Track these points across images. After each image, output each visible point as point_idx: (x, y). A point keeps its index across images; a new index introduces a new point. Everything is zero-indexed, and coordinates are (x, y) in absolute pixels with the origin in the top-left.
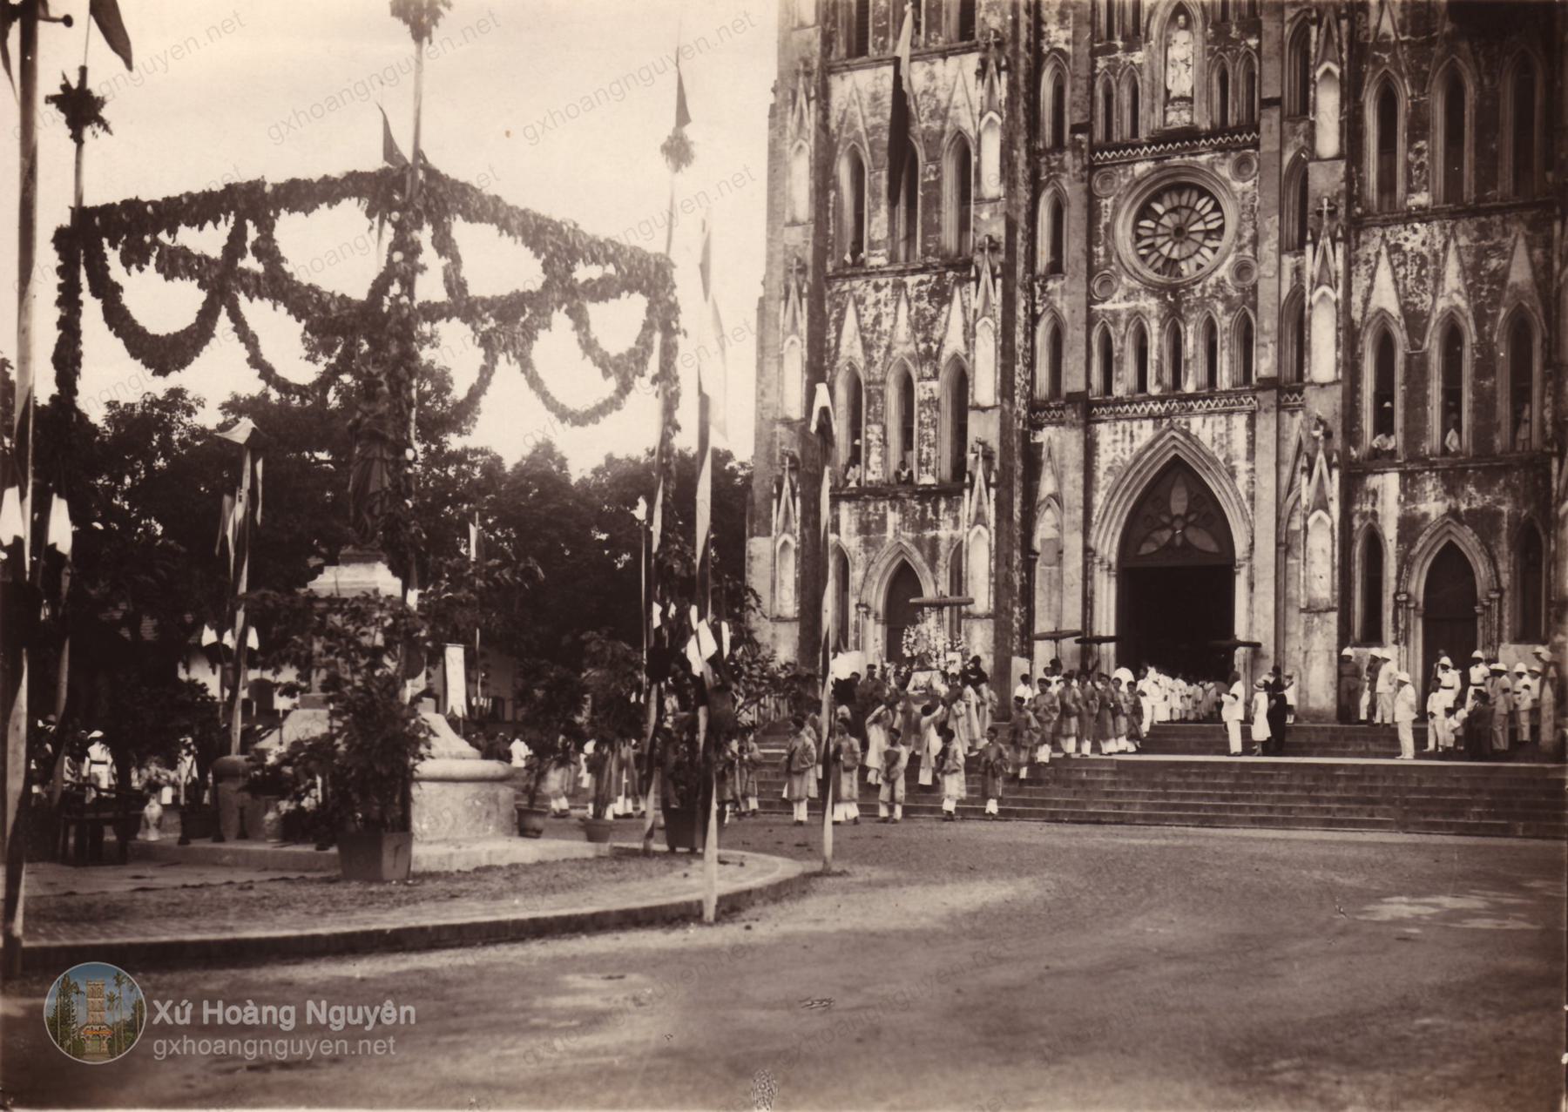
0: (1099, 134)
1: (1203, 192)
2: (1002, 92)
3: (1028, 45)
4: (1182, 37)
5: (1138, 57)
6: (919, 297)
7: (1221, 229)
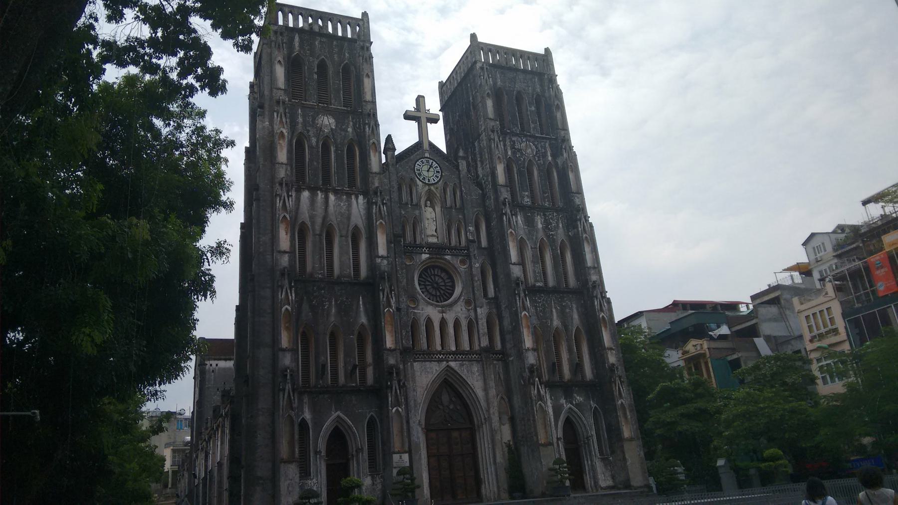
4: (430, 210)
5: (417, 212)
7: (453, 287)
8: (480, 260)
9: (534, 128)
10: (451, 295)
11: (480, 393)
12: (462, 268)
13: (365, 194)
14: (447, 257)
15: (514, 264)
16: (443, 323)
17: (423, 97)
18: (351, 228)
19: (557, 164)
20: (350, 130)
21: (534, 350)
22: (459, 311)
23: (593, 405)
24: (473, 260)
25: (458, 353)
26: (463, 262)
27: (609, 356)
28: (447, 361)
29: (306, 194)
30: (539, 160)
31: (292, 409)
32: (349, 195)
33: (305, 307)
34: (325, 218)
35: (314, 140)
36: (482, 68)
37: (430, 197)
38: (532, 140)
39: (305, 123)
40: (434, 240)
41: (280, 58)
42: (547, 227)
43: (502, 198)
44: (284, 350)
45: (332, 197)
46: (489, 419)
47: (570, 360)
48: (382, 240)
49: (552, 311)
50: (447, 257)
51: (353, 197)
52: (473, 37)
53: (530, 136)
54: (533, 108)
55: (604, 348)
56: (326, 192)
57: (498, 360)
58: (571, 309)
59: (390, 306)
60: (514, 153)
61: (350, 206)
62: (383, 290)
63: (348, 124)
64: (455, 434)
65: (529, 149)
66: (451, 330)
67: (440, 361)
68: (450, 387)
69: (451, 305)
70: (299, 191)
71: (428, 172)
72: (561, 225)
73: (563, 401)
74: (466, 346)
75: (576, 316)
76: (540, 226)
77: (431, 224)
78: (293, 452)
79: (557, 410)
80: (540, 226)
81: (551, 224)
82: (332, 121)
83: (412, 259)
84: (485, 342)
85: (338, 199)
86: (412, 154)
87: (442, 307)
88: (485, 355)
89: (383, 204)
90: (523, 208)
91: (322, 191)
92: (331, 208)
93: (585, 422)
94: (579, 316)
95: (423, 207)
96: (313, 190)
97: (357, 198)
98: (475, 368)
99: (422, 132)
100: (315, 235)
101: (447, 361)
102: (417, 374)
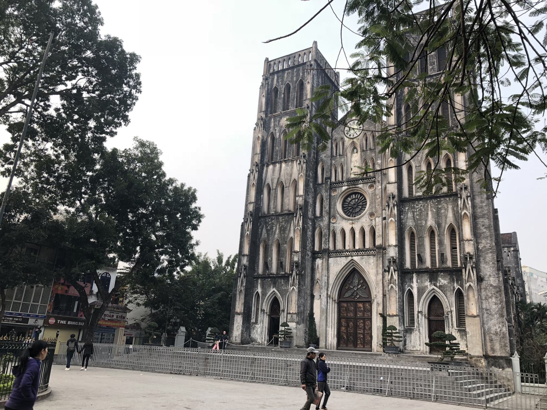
0: (333, 180)
2: (304, 166)
3: (314, 157)
5: (343, 160)
6: (282, 222)
7: (366, 204)
9: (432, 68)
12: (371, 191)
14: (360, 186)
15: (392, 183)
16: (353, 231)
21: (395, 246)
23: (457, 286)
24: (377, 184)
25: (363, 251)
26: (371, 187)
29: (271, 167)
35: (278, 134)
37: (354, 147)
39: (274, 127)
41: (264, 94)
44: (244, 256)
45: (283, 165)
49: (427, 214)
50: (360, 186)
51: (295, 162)
55: (463, 240)
58: (447, 210)
61: (292, 168)
62: (296, 216)
64: (361, 305)
67: (347, 256)
69: (358, 219)
70: (268, 166)
73: (427, 283)
75: (450, 215)
79: (421, 291)
84: (379, 242)
87: (352, 220)
89: (304, 163)
95: (349, 155)
96: (274, 164)
97: (297, 161)
101: (352, 256)
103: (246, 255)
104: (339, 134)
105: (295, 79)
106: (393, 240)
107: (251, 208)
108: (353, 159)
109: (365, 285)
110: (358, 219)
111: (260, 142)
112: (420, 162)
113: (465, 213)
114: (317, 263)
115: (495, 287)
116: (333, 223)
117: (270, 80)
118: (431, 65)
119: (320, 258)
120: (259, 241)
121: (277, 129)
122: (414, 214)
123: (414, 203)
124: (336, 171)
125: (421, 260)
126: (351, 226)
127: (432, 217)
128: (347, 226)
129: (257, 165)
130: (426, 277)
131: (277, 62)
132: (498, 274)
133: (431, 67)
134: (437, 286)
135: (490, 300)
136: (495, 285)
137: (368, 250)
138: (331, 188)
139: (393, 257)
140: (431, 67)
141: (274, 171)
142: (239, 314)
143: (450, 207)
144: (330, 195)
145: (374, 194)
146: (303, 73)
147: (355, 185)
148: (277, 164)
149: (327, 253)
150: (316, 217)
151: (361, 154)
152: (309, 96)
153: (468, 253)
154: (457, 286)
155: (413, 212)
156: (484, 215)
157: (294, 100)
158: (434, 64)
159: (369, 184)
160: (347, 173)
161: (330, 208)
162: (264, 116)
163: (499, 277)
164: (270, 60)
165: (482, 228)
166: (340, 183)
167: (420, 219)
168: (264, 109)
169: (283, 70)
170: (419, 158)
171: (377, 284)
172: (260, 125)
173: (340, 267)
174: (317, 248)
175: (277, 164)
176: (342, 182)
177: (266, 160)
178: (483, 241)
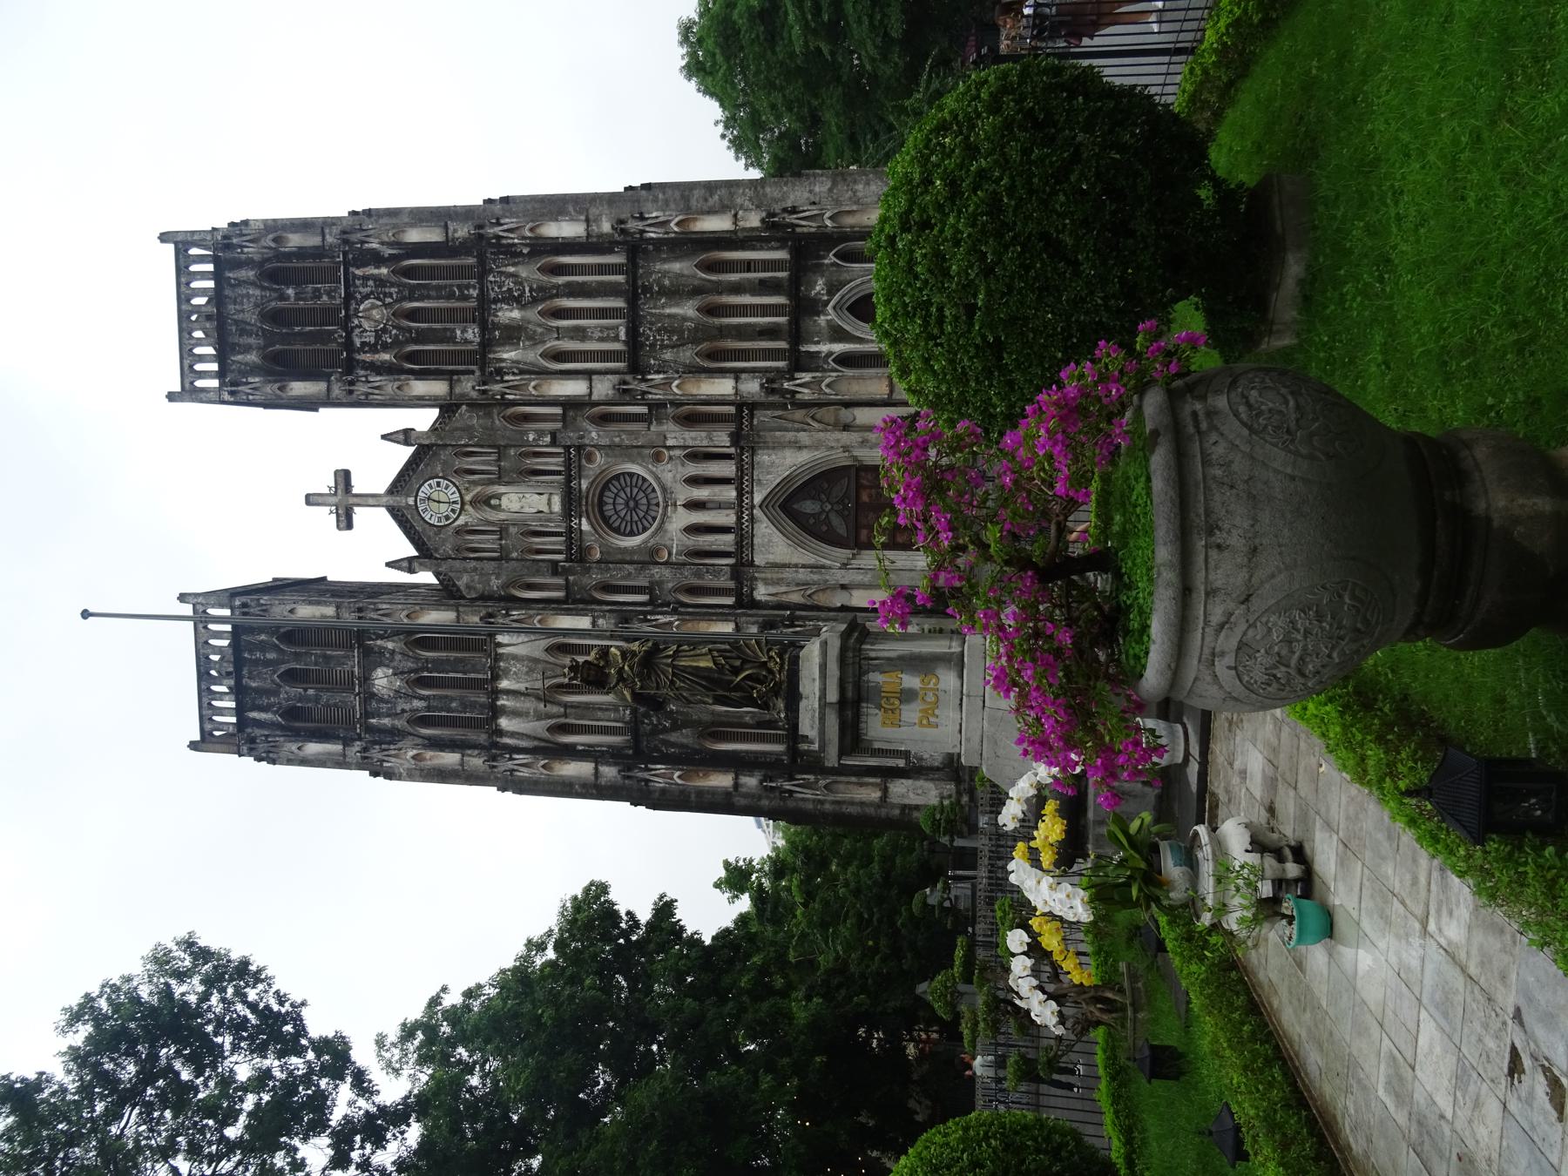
1: (606, 487)
4: (505, 502)
5: (513, 530)
7: (631, 475)
8: (587, 425)
9: (328, 294)
10: (644, 480)
11: (804, 457)
12: (599, 458)
13: (492, 635)
14: (584, 485)
15: (591, 387)
17: (308, 496)
18: (552, 659)
19: (394, 259)
20: (390, 645)
21: (737, 379)
22: (672, 473)
23: (831, 258)
24: (587, 441)
25: (742, 482)
26: (590, 458)
27: (748, 225)
28: (753, 507)
29: (504, 723)
30: (391, 295)
31: (817, 781)
32: (498, 658)
33: (673, 737)
34: (538, 698)
36: (232, 393)
37: (484, 501)
38: (354, 306)
40: (556, 500)
41: (294, 747)
42: (518, 300)
43: (474, 394)
44: (736, 785)
45: (504, 684)
46: (846, 449)
47: (754, 293)
48: (565, 622)
49: (669, 316)
50: (584, 485)
51: (501, 651)
52: (172, 397)
53: (347, 310)
54: (290, 292)
55: (735, 232)
56: (497, 693)
57: (752, 416)
58: (665, 274)
59: (671, 623)
60: (386, 347)
61: (515, 657)
63: (380, 647)
64: (865, 498)
65: (371, 317)
66: (703, 493)
67: (752, 519)
68: (791, 504)
69: (664, 489)
70: (500, 732)
71: (440, 500)
72: (511, 269)
73: (822, 320)
74: (727, 469)
75: (676, 267)
76: (516, 314)
77: (526, 502)
78: (872, 784)
79: (838, 334)
80: (516, 314)
81: (510, 290)
82: (380, 672)
83: (590, 548)
84: (721, 439)
85: (506, 672)
86: (412, 526)
88: (745, 443)
89: (508, 615)
90: (487, 345)
91: (497, 699)
92: (521, 686)
93: (858, 281)
94: (677, 259)
95: (502, 516)
96: (497, 712)
97: (500, 645)
98: (763, 457)
99: (369, 500)
100: (565, 715)
101: (753, 507)
102: (771, 558)
103: (736, 778)
104: (444, 541)
105: (271, 656)
106: (723, 387)
107: (609, 772)
108: (515, 506)
109: (818, 483)
110: (664, 489)
111: (429, 754)
112: (549, 329)
113: (677, 224)
114: (763, 598)
115: (834, 184)
116: (670, 554)
117: (258, 732)
118: (319, 297)
119: (753, 590)
120: (697, 752)
121: (402, 705)
122: (667, 347)
123: (643, 345)
124: (539, 552)
125: (770, 333)
126: (680, 509)
127: (677, 305)
128: (681, 518)
129: (494, 758)
130: (807, 324)
131: (206, 712)
132: (808, 176)
133: (325, 298)
134: (828, 302)
135: (860, 194)
136: (829, 184)
137: (740, 468)
138: (582, 560)
139: (762, 386)
140: (325, 298)
141: (515, 714)
142: (885, 791)
143: (658, 266)
144: (598, 562)
145: (610, 448)
146: (261, 630)
147: (580, 498)
148: (499, 703)
149: (743, 568)
150: (651, 602)
151: (507, 484)
152: (330, 611)
153: (763, 221)
154: (831, 258)
155: (663, 347)
156: (683, 196)
157: (331, 657)
158: (318, 290)
159: (584, 462)
160: (549, 520)
161: (631, 563)
162: (358, 745)
163: (815, 176)
164: (197, 737)
165: (711, 202)
166: (570, 534)
167: (680, 332)
168: (336, 748)
169: (238, 691)
170: (539, 330)
171: (815, 447)
172: (380, 756)
173: (777, 537)
174: (730, 601)
175: (499, 703)
176: (570, 529)
177: (482, 738)
178: (739, 201)
